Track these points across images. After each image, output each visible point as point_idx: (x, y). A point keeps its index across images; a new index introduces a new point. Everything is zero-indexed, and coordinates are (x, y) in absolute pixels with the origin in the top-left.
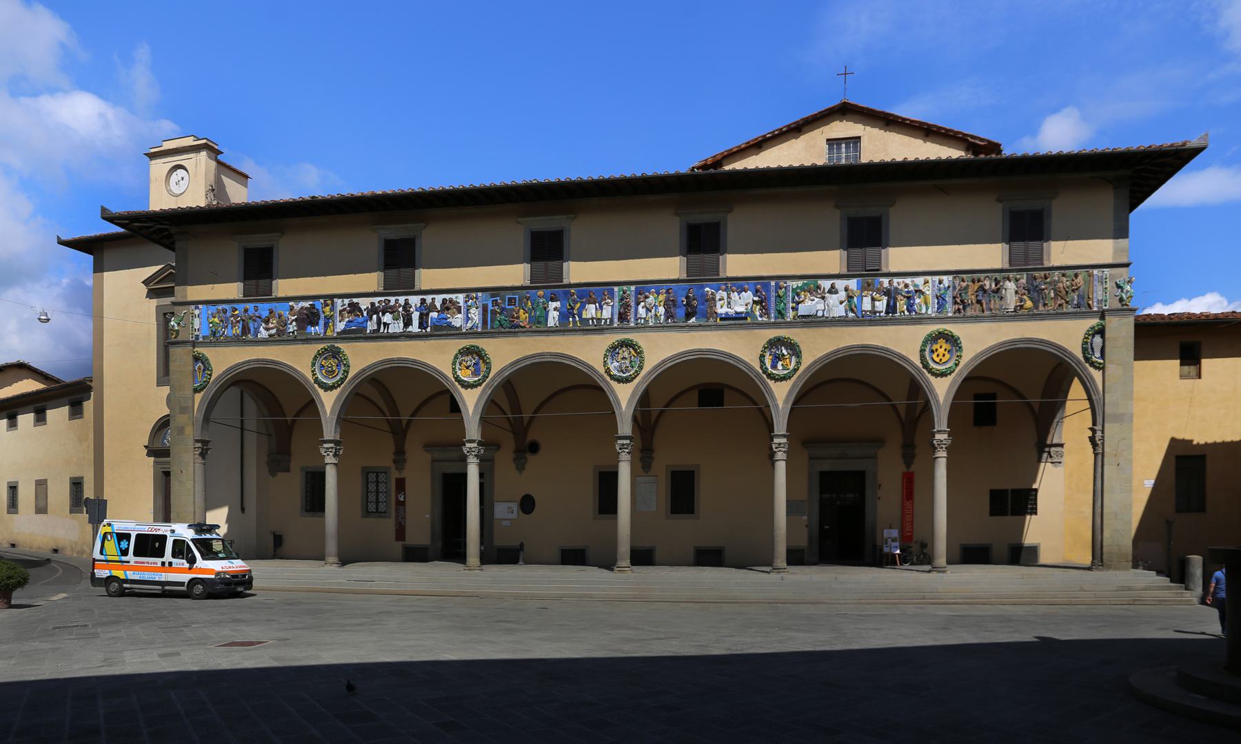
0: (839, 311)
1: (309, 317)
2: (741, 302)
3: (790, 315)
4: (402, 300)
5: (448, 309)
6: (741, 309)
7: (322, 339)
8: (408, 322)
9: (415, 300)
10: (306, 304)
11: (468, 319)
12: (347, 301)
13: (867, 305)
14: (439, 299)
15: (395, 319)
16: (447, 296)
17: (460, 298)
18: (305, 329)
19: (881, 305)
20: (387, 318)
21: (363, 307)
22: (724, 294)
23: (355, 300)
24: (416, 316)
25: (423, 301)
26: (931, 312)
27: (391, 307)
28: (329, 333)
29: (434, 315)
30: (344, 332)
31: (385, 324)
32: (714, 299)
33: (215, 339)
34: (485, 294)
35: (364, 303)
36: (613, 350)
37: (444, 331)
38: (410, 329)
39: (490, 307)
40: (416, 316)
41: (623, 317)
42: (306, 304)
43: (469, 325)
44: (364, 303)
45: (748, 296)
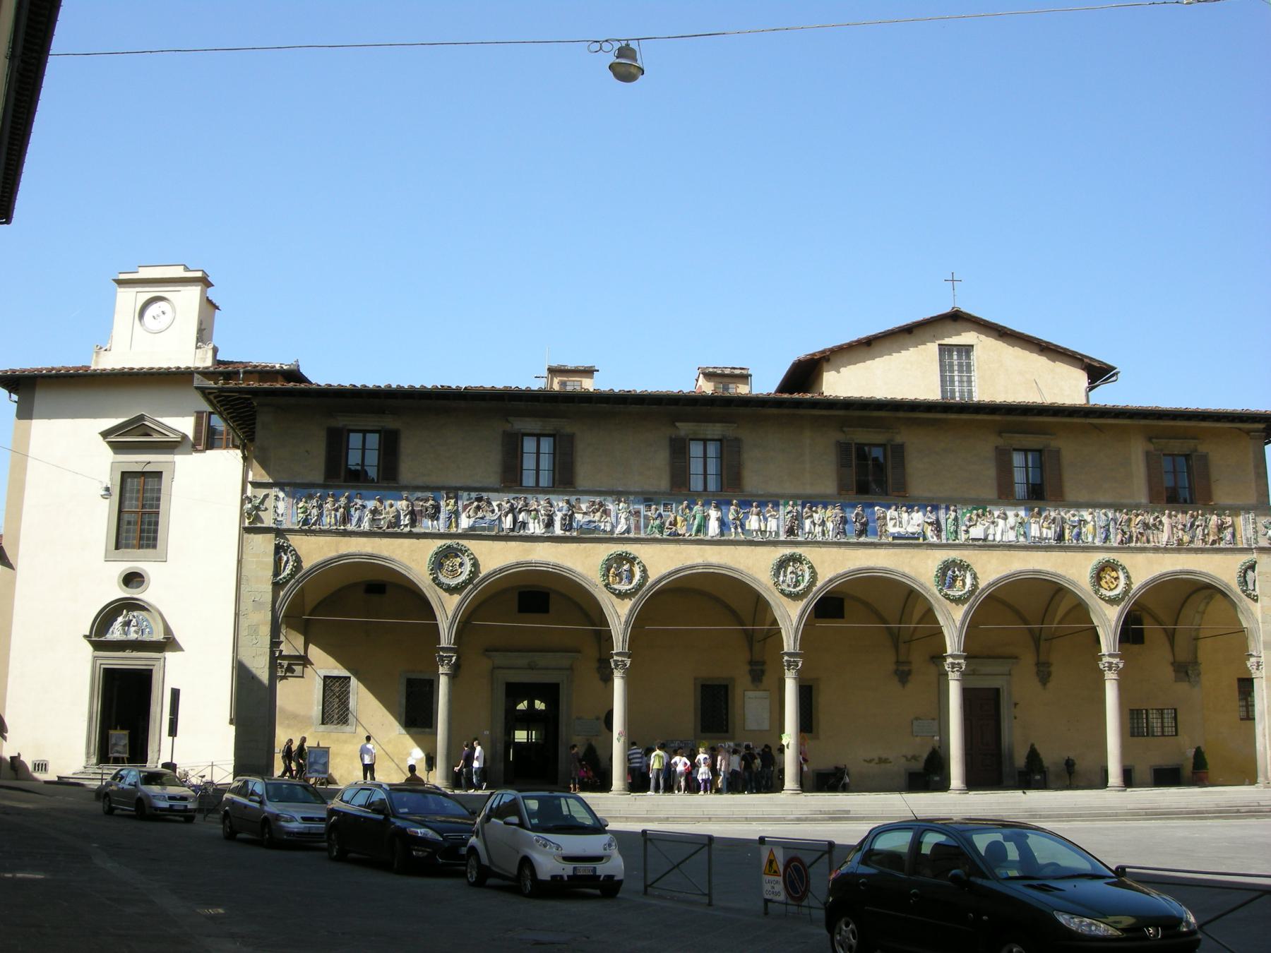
0: (1011, 537)
2: (913, 521)
3: (963, 537)
6: (911, 529)
8: (549, 524)
13: (1034, 531)
19: (1050, 534)
22: (895, 514)
26: (1098, 543)
28: (453, 530)
30: (472, 528)
32: (885, 518)
33: (307, 528)
36: (782, 564)
41: (791, 531)
45: (918, 517)
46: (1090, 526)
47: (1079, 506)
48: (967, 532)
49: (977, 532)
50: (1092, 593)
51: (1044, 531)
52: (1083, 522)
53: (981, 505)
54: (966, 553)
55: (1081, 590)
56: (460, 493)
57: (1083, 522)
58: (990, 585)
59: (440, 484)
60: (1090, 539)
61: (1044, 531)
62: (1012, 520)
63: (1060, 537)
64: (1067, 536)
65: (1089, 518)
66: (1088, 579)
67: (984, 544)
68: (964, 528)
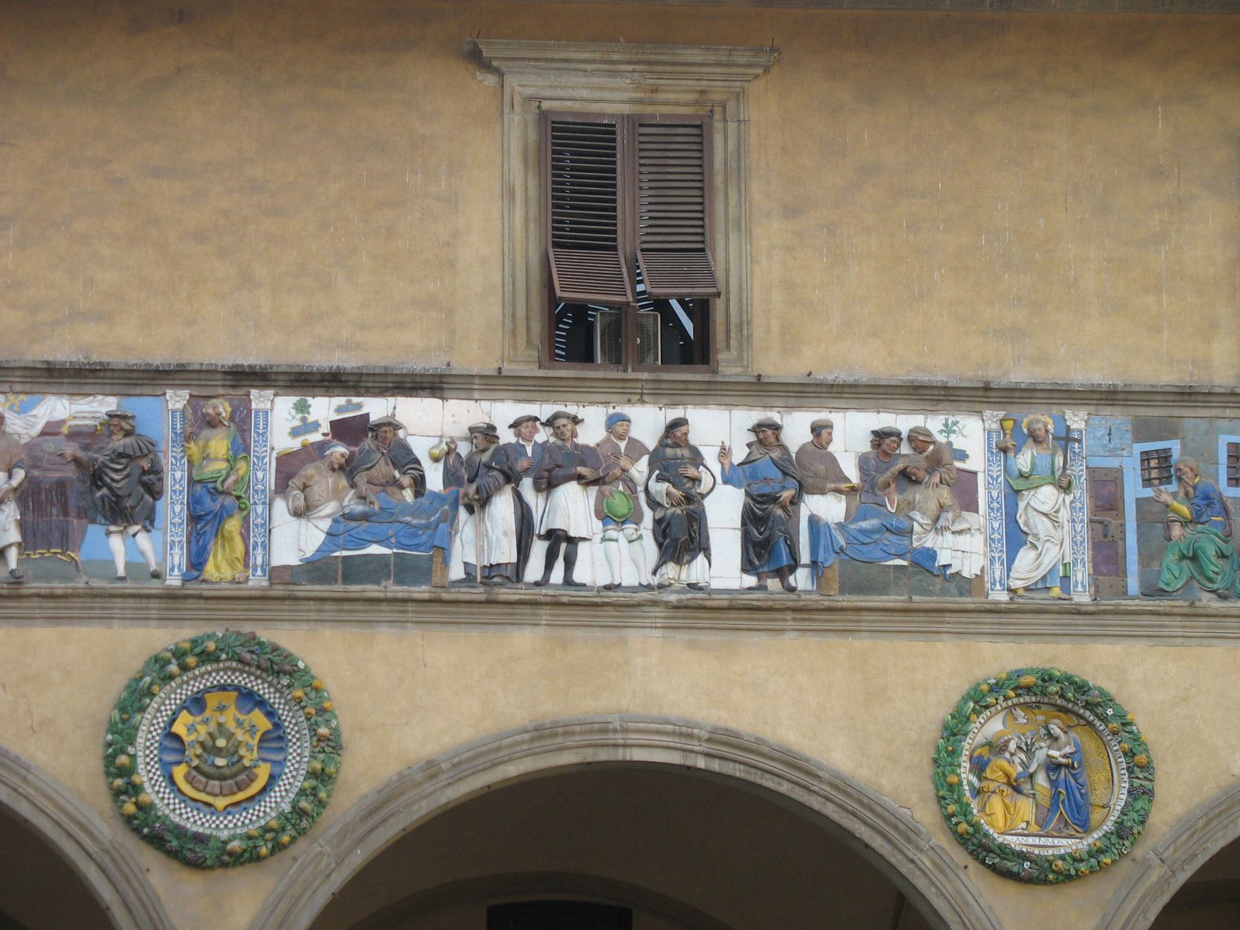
1: (107, 482)
4: (647, 421)
5: (907, 478)
7: (171, 596)
8: (682, 537)
9: (719, 430)
10: (94, 407)
11: (1016, 539)
12: (325, 409)
14: (851, 433)
15: (605, 515)
16: (904, 422)
17: (970, 436)
18: (65, 541)
20: (572, 507)
21: (421, 448)
23: (376, 408)
24: (724, 511)
25: (766, 434)
27: (585, 455)
29: (828, 508)
30: (316, 569)
31: (556, 537)
34: (1119, 418)
35: (427, 424)
37: (886, 586)
38: (697, 570)
39: (1133, 489)
40: (724, 511)
42: (94, 407)
43: (1026, 566)
44: (427, 424)
56: (259, 399)
59: (160, 356)
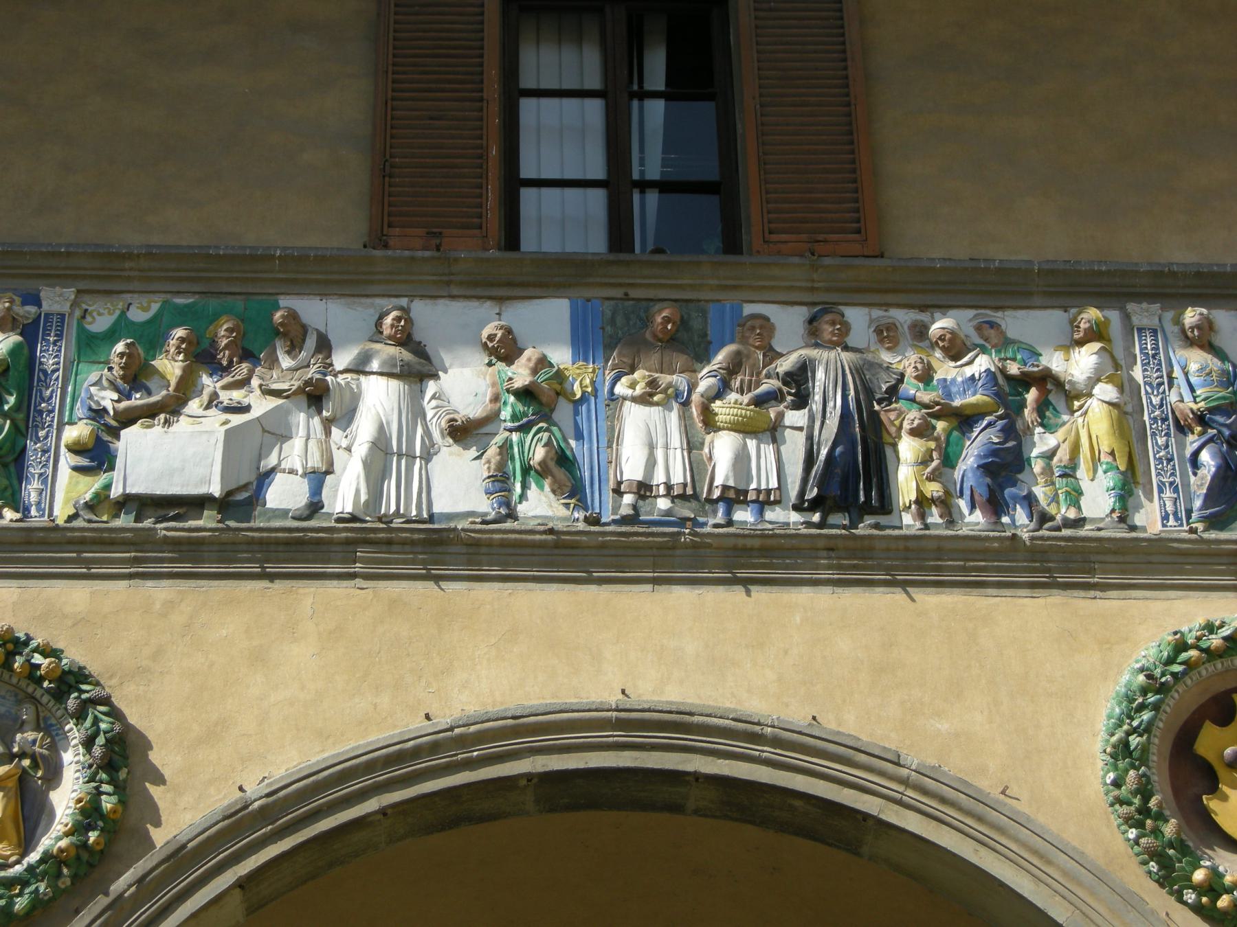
19: (781, 464)
46: (1095, 419)
47: (993, 288)
48: (97, 455)
49: (174, 455)
50: (1138, 879)
51: (723, 449)
52: (1029, 392)
53: (234, 310)
54: (75, 596)
55: (1041, 851)
57: (1057, 393)
58: (242, 825)
60: (1098, 499)
61: (723, 447)
62: (465, 384)
63: (851, 477)
64: (906, 480)
65: (1080, 364)
66: (1094, 773)
67: (223, 537)
68: (77, 431)
